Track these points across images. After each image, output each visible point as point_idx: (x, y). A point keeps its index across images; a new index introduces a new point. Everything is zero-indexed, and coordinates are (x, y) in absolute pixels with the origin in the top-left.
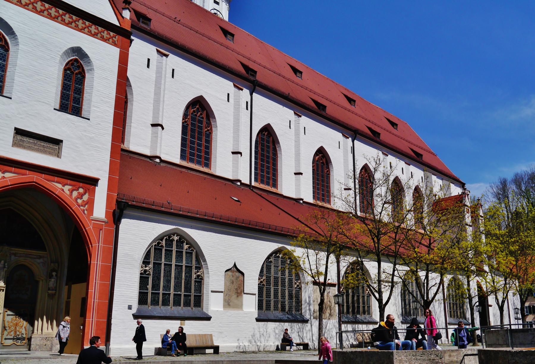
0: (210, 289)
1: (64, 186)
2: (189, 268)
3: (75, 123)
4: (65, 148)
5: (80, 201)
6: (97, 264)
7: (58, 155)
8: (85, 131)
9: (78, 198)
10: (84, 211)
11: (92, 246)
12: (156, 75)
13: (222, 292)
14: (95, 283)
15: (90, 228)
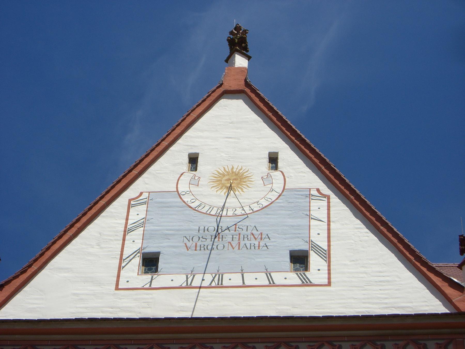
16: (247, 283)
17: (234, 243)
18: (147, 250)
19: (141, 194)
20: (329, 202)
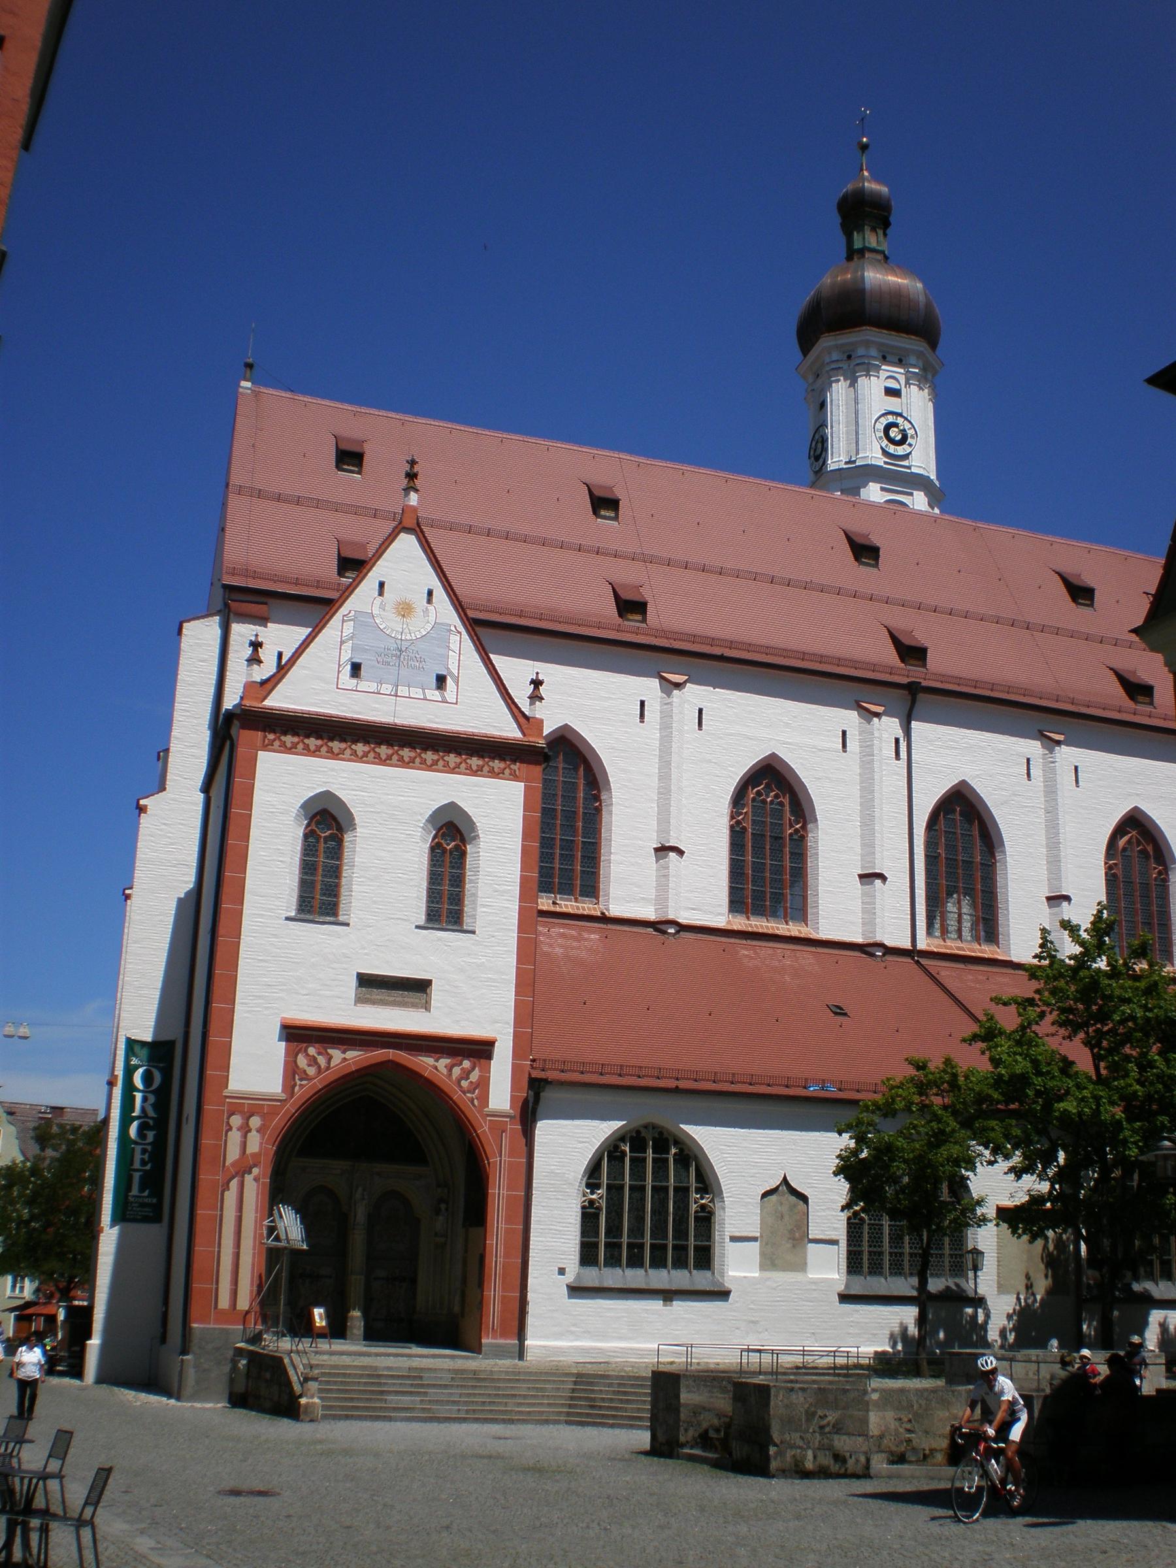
0: (726, 1233)
1: (437, 1061)
2: (682, 1192)
3: (450, 944)
4: (436, 993)
5: (464, 1084)
6: (499, 1194)
7: (427, 1007)
8: (469, 954)
9: (462, 1078)
10: (472, 1101)
11: (489, 1163)
12: (660, 733)
13: (755, 1239)
14: (498, 1227)
15: (484, 1129)
16: (411, 696)
17: (405, 663)
18: (353, 660)
19: (350, 611)
20: (461, 638)
